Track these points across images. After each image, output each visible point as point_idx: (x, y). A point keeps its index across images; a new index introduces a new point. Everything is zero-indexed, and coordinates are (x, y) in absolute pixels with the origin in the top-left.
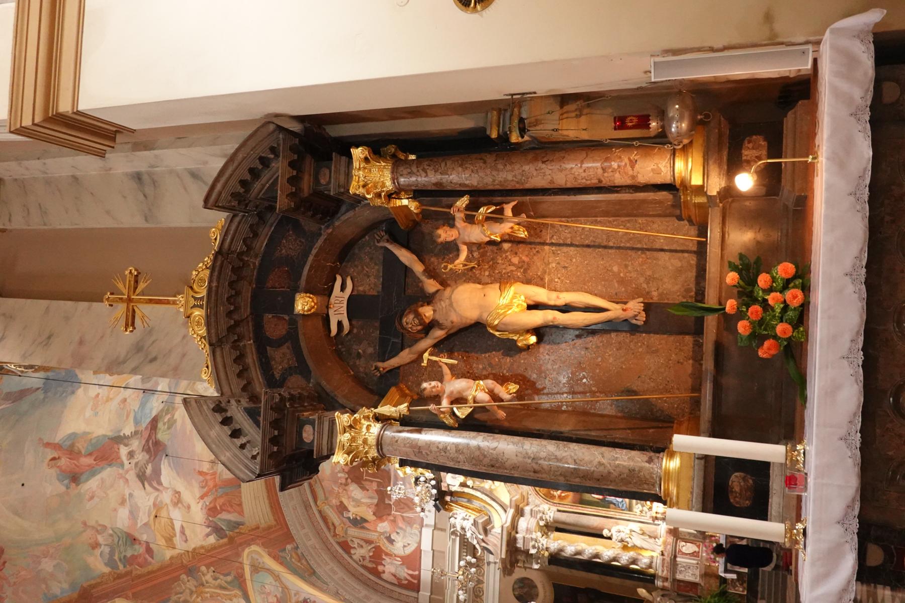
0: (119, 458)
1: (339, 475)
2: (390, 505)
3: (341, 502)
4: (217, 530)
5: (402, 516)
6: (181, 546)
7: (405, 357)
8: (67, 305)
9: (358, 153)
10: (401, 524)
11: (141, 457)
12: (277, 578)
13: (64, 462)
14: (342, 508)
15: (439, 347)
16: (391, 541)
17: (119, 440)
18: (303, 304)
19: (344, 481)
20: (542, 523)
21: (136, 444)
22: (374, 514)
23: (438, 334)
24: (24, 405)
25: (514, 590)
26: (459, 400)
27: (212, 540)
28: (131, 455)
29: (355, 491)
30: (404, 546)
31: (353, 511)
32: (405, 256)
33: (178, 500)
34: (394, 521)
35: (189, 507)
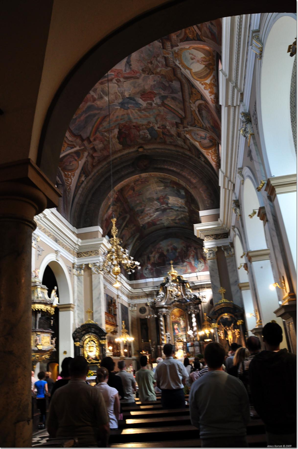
0: (163, 205)
1: (161, 250)
2: (156, 267)
3: (153, 252)
4: (143, 225)
5: (153, 272)
6: (140, 221)
7: (223, 326)
8: (218, 273)
9: (242, 320)
10: (152, 271)
11: (163, 208)
12: (132, 242)
13: (162, 197)
14: (151, 253)
15: (224, 330)
16: (146, 269)
17: (167, 204)
18: (226, 314)
19: (159, 251)
20: (165, 314)
21: (166, 207)
22: (153, 263)
23: (226, 330)
24: (176, 192)
25: (142, 307)
26: (221, 334)
27: (141, 225)
28: (163, 206)
29: (157, 256)
30: (145, 273)
31: (151, 256)
32: (233, 324)
33: (151, 216)
34: (152, 269)
35: (149, 219)
